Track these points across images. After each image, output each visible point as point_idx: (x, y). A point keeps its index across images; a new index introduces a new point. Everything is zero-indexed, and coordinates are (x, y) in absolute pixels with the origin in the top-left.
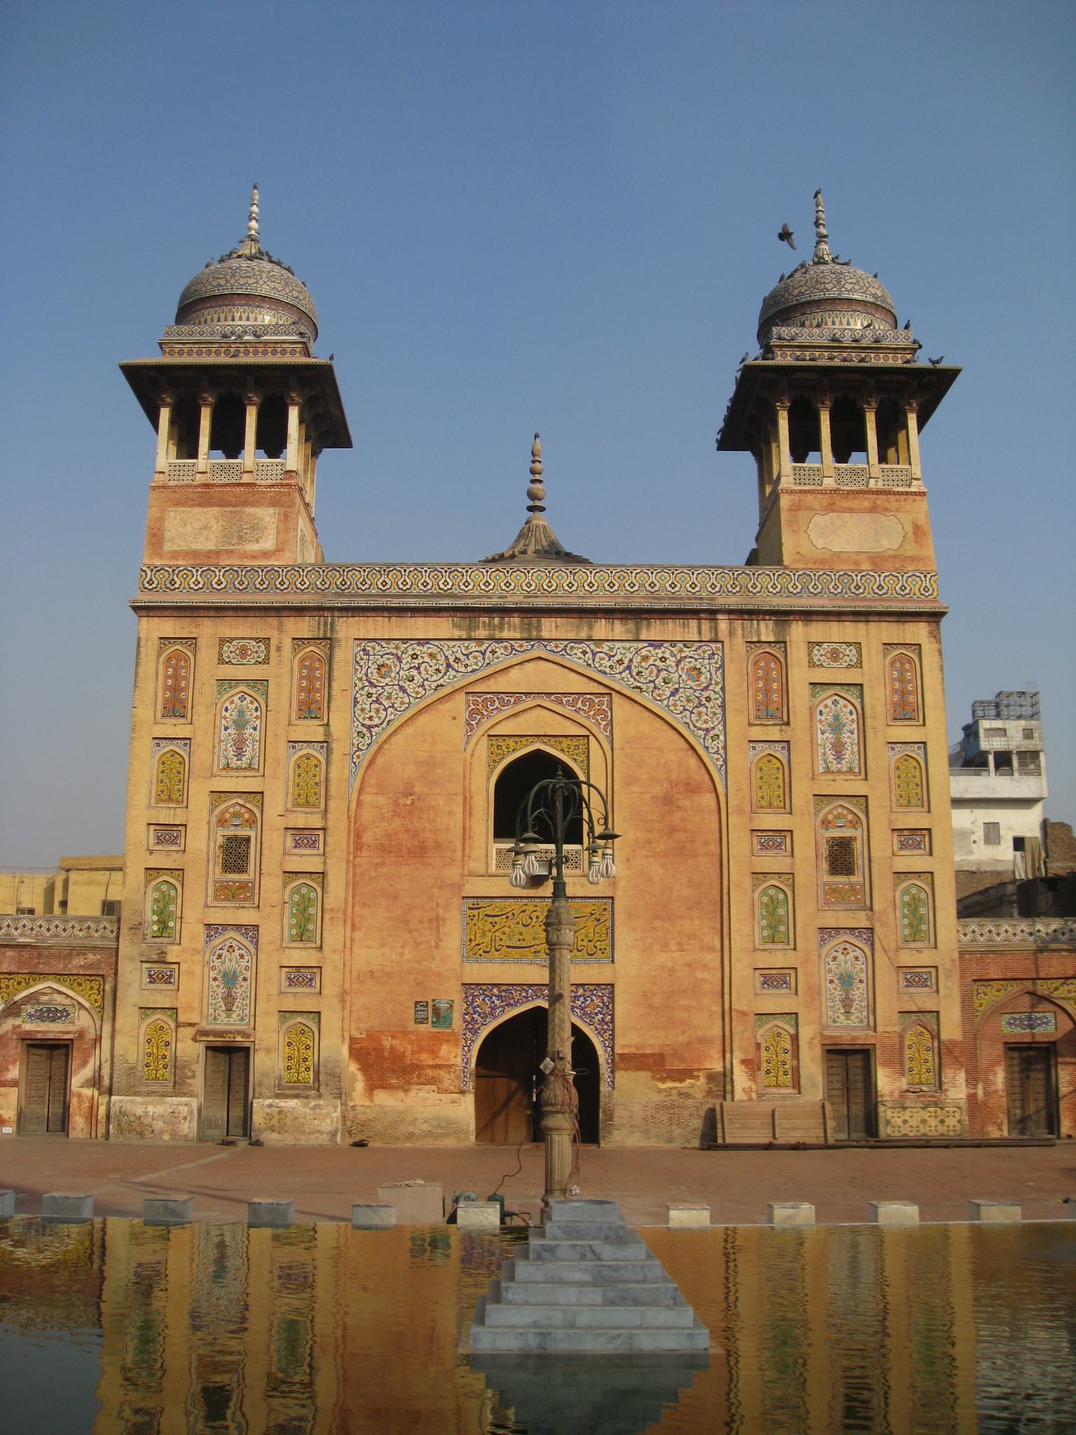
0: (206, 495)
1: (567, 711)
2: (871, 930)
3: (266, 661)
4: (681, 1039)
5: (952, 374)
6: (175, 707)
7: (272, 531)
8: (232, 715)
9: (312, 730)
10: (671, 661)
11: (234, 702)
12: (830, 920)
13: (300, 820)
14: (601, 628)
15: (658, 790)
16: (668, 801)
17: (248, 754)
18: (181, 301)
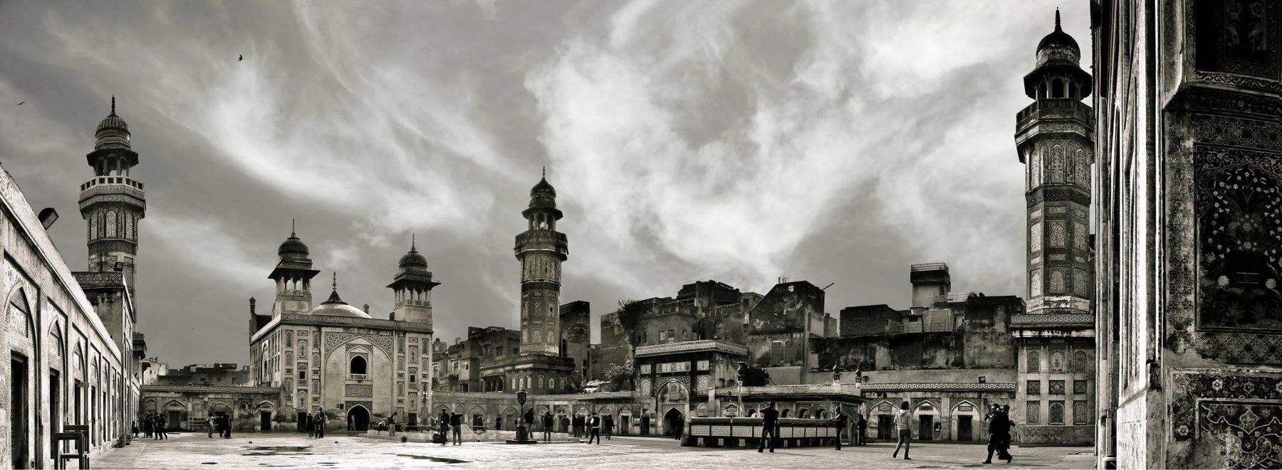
6: (289, 344)
9: (316, 350)
13: (315, 369)
14: (372, 332)
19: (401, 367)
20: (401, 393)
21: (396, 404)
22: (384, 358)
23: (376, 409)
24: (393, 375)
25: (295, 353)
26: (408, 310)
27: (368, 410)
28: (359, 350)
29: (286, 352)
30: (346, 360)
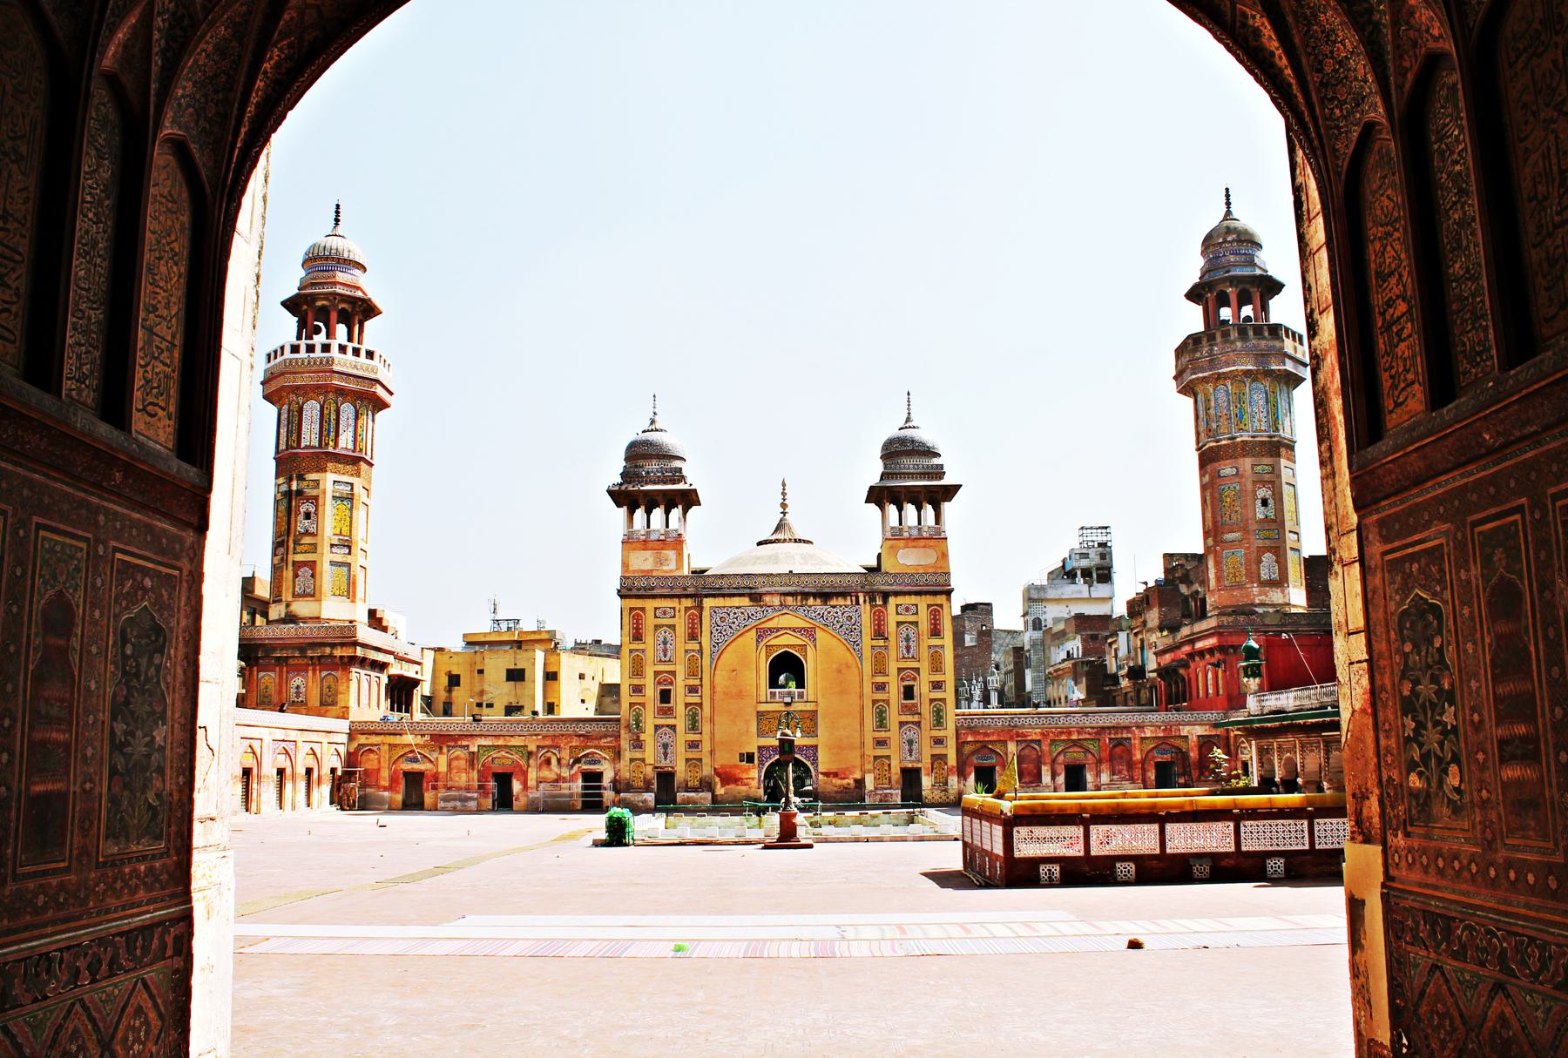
0: (645, 544)
1: (798, 635)
2: (919, 722)
3: (674, 617)
4: (844, 766)
5: (959, 486)
6: (637, 636)
7: (674, 561)
8: (661, 639)
9: (694, 646)
10: (840, 613)
11: (661, 635)
12: (904, 718)
13: (691, 682)
14: (811, 601)
15: (834, 666)
16: (839, 671)
17: (669, 654)
18: (626, 453)
19: (879, 669)
20: (881, 723)
21: (870, 751)
22: (841, 652)
23: (825, 762)
24: (862, 686)
25: (650, 655)
26: (891, 547)
27: (808, 764)
28: (786, 641)
29: (631, 651)
30: (757, 662)
